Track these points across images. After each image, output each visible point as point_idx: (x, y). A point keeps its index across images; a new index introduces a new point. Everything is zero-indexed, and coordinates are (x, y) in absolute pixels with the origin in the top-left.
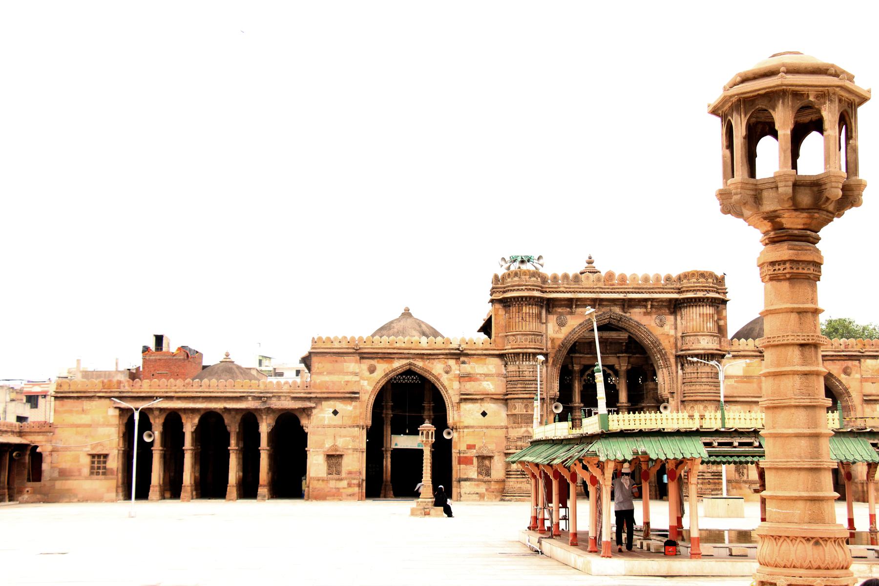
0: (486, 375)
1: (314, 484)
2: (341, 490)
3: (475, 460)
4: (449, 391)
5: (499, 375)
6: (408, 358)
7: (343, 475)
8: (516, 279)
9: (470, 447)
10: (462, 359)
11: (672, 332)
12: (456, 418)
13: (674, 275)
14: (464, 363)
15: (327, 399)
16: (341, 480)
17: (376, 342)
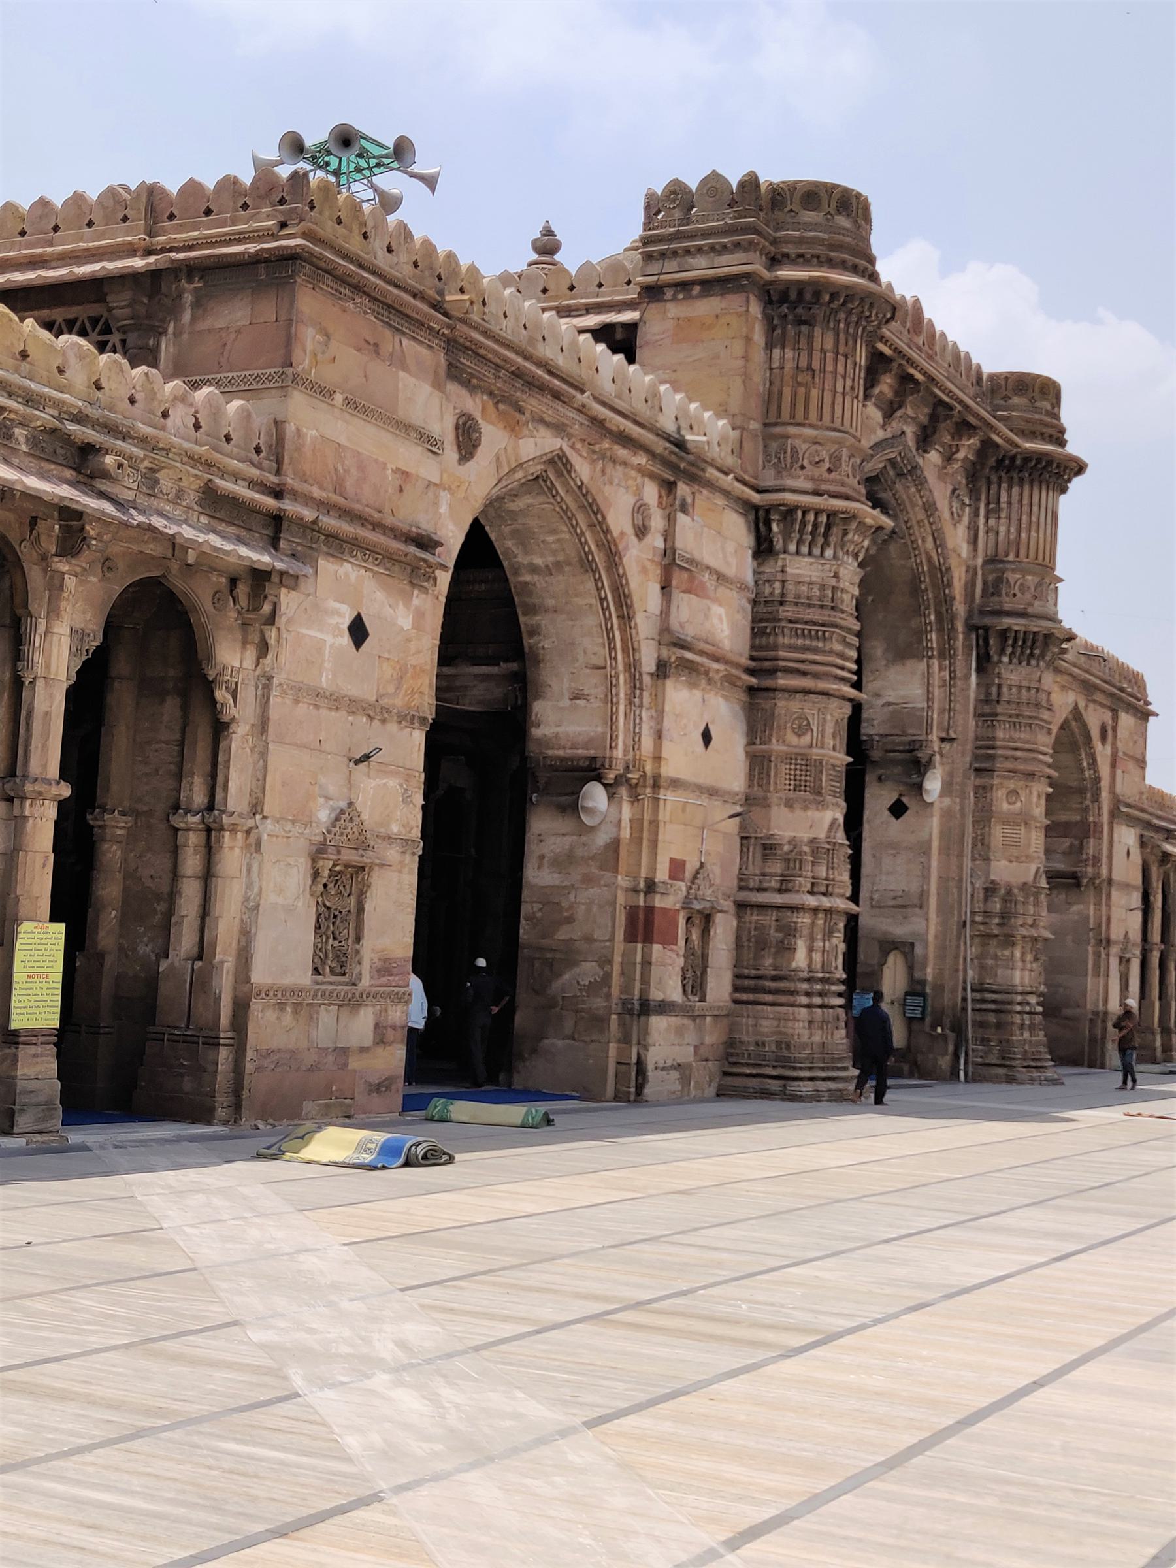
0: (721, 577)
1: (269, 1029)
2: (354, 1063)
3: (682, 922)
4: (639, 619)
5: (743, 587)
6: (559, 429)
7: (365, 982)
8: (843, 221)
9: (677, 868)
10: (683, 489)
11: (964, 550)
12: (647, 743)
13: (988, 369)
14: (684, 508)
15: (340, 546)
16: (353, 1003)
17: (492, 307)
